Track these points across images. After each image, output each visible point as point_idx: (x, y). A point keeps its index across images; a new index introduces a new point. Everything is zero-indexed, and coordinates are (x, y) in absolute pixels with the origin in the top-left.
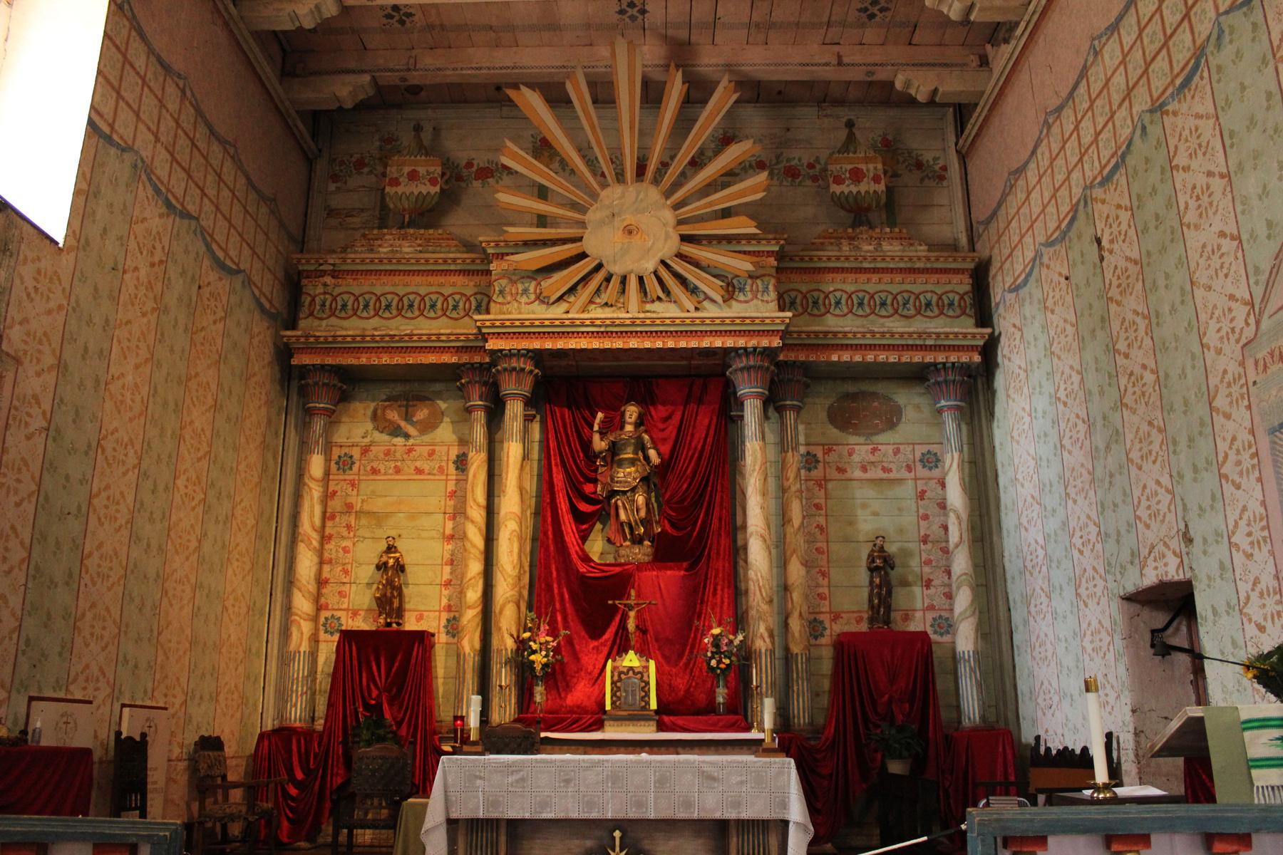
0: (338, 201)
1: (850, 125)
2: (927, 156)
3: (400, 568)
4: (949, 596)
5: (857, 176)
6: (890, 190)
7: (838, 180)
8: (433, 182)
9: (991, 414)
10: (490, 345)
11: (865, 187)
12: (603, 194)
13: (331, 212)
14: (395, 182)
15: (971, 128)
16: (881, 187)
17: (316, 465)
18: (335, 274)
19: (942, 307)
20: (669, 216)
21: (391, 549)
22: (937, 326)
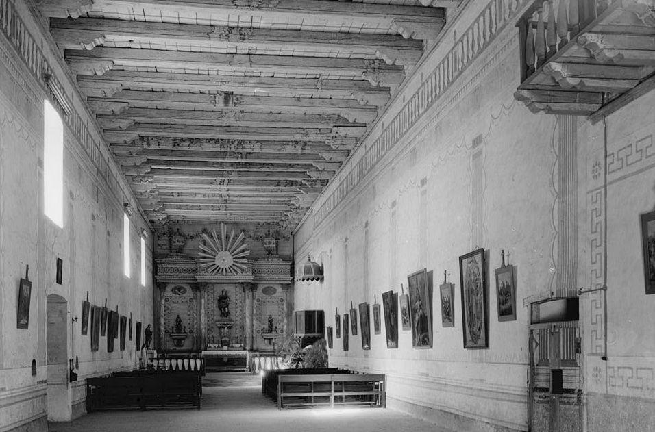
0: (160, 242)
1: (269, 231)
2: (286, 235)
3: (180, 321)
4: (283, 326)
5: (270, 243)
6: (277, 247)
7: (266, 244)
8: (183, 242)
9: (295, 292)
10: (198, 281)
11: (271, 245)
12: (219, 253)
13: (159, 245)
14: (174, 242)
15: (293, 233)
16: (274, 245)
17: (163, 301)
18: (164, 263)
19: (285, 272)
20: (232, 258)
21: (178, 317)
22: (282, 276)
